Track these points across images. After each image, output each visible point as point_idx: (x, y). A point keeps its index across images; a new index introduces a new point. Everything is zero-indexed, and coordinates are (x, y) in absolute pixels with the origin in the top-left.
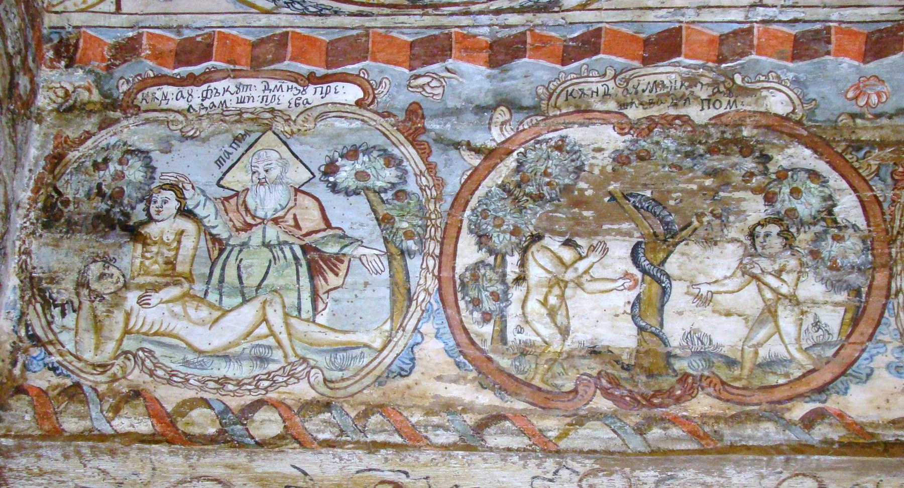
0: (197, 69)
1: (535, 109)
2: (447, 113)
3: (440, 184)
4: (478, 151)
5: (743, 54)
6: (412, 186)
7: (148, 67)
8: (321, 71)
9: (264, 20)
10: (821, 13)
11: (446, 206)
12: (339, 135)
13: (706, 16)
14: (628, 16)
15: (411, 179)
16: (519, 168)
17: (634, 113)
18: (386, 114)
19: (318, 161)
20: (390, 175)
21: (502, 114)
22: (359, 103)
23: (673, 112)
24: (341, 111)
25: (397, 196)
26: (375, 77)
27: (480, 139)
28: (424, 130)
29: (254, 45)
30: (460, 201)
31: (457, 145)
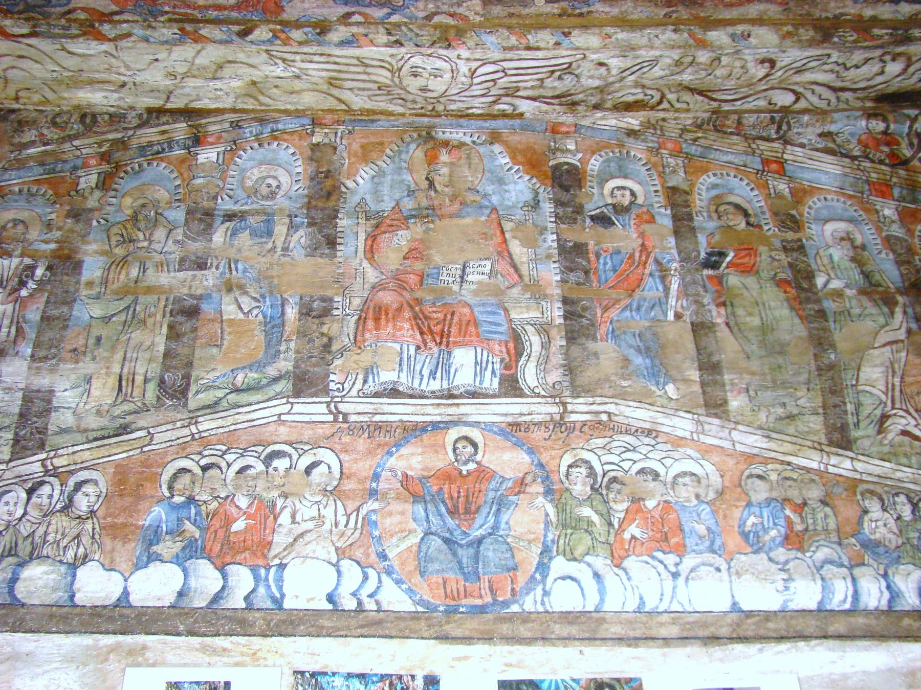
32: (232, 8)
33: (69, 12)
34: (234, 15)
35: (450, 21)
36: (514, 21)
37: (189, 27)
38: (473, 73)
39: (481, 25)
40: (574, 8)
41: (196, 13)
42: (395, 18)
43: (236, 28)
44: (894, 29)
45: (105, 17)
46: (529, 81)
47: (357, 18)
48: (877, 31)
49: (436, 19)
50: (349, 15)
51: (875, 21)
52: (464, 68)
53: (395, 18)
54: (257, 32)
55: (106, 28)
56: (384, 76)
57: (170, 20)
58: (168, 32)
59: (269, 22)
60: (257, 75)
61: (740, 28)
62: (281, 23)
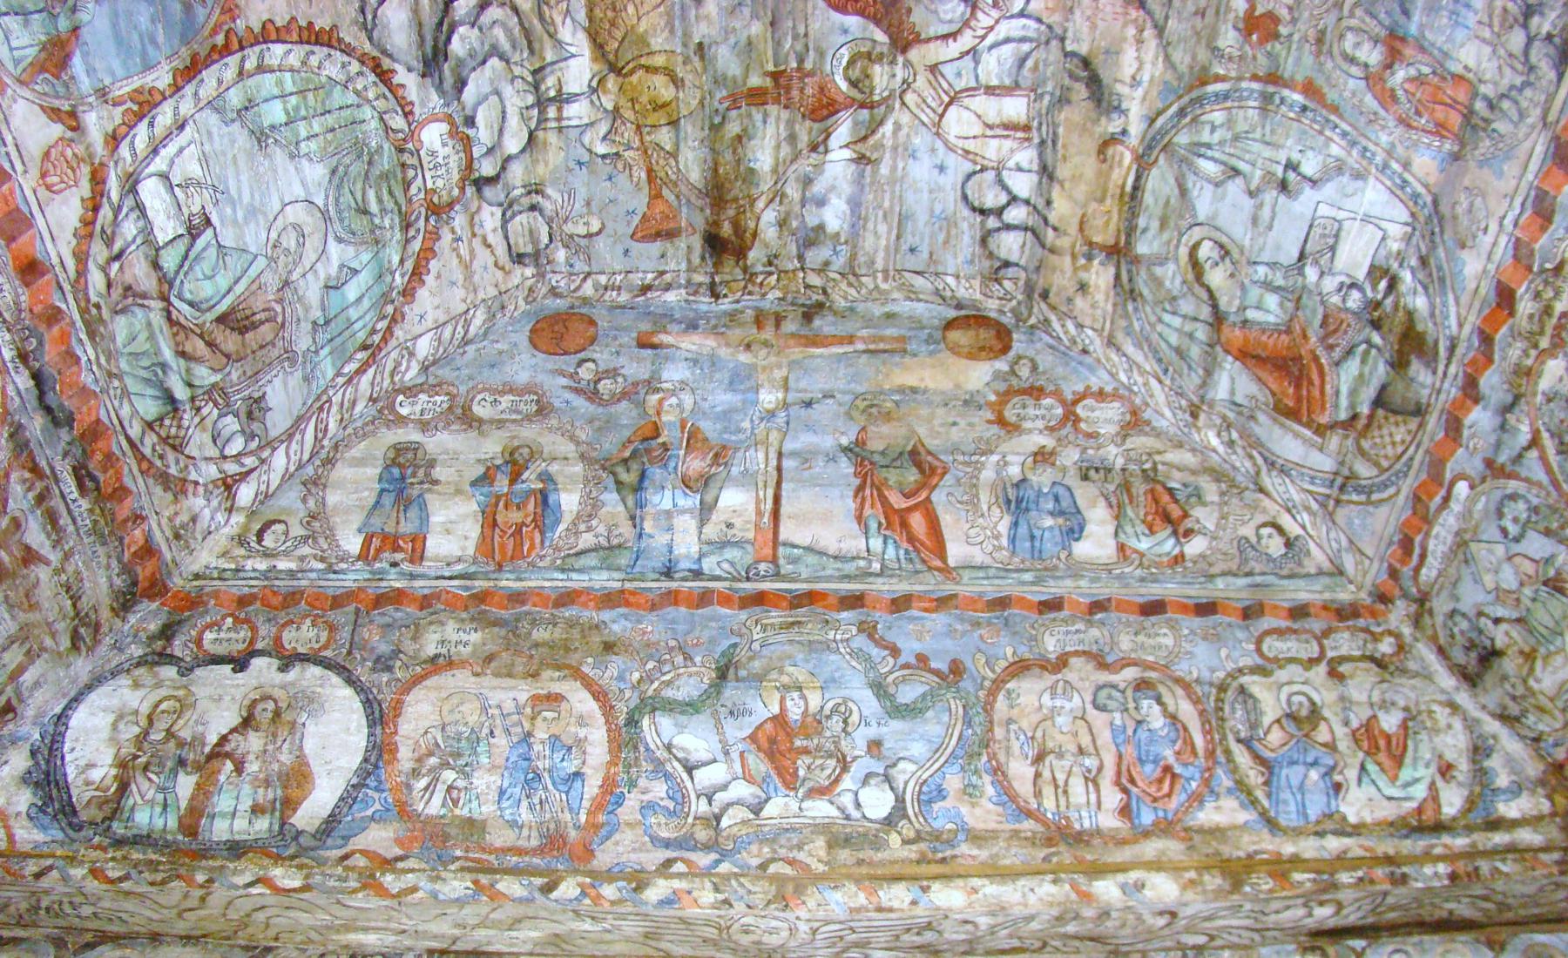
0: (1417, 551)
1: (1517, 398)
2: (1498, 445)
3: (1539, 485)
4: (1528, 448)
5: (1532, 252)
6: (1535, 501)
7: (1406, 571)
8: (1443, 492)
9: (1401, 498)
10: (1524, 185)
11: (1554, 494)
12: (1486, 510)
13: (1497, 257)
14: (1477, 305)
15: (1530, 497)
16: (1552, 436)
17: (1544, 343)
18: (1483, 480)
19: (1498, 536)
20: (1521, 506)
21: (1511, 418)
22: (1472, 487)
23: (1554, 320)
24: (1471, 500)
25: (1537, 513)
26: (1458, 469)
27: (1524, 434)
28: (1503, 466)
29: (1414, 513)
30: (1555, 483)
31: (1520, 456)
32: (534, 852)
33: (346, 857)
34: (536, 861)
35: (787, 870)
36: (864, 870)
37: (484, 880)
38: (814, 931)
39: (822, 877)
40: (935, 851)
41: (492, 858)
42: (724, 867)
43: (538, 881)
44: (1318, 872)
45: (388, 864)
46: (883, 938)
47: (679, 867)
48: (1297, 876)
49: (772, 869)
50: (669, 863)
51: (1296, 861)
52: (803, 927)
53: (724, 867)
54: (563, 887)
55: (388, 880)
56: (711, 933)
57: (462, 869)
58: (456, 886)
59: (576, 872)
60: (559, 929)
61: (1133, 876)
62: (591, 874)
